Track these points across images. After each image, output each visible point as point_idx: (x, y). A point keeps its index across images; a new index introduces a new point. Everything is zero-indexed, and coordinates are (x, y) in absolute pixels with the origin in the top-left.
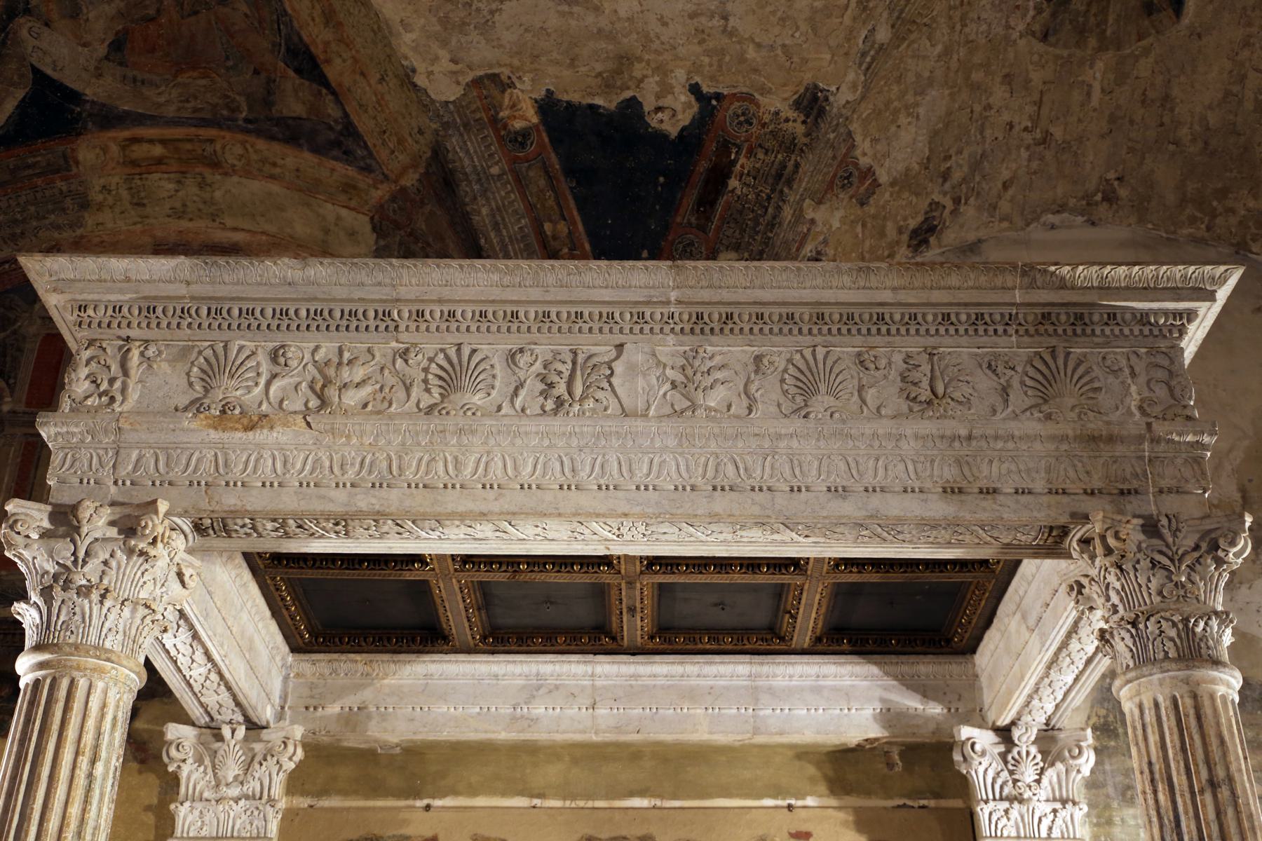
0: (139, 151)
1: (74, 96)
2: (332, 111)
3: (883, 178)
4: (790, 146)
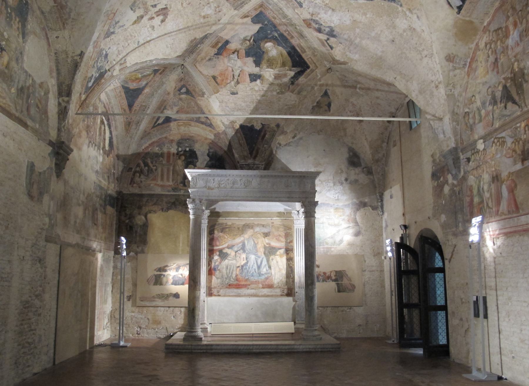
0: (179, 124)
1: (171, 118)
2: (208, 121)
3: (288, 131)
4: (275, 131)
